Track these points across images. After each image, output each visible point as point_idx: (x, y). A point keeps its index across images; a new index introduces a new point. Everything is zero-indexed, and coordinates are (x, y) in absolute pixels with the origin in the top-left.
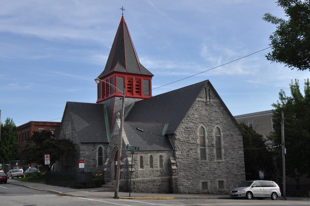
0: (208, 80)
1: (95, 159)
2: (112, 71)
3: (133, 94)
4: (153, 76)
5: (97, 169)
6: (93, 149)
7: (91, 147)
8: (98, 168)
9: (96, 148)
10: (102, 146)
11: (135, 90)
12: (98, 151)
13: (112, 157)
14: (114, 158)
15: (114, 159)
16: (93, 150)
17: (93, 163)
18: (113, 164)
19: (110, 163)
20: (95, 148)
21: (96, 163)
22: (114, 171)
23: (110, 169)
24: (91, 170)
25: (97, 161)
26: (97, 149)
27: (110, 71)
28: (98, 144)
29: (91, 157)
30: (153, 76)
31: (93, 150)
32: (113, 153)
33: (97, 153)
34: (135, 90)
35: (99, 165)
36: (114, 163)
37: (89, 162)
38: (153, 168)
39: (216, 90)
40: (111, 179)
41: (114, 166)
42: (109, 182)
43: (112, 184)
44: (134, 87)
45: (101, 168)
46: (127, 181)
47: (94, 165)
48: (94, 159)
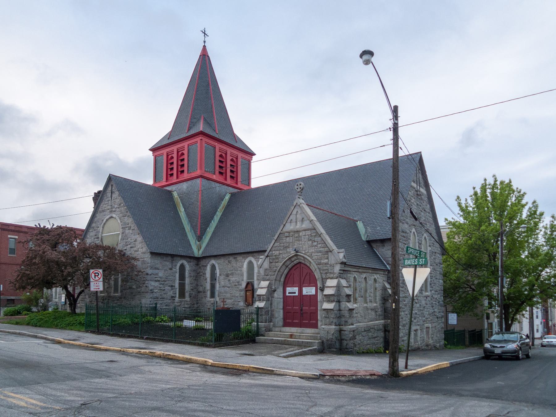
0: (421, 152)
1: (174, 286)
2: (192, 132)
3: (226, 179)
4: (255, 154)
5: (177, 304)
6: (170, 267)
7: (168, 263)
8: (178, 303)
9: (176, 266)
10: (185, 262)
11: (229, 174)
12: (178, 271)
13: (278, 279)
14: (282, 280)
15: (282, 282)
16: (171, 269)
17: (171, 293)
18: (279, 294)
19: (271, 291)
20: (174, 264)
21: (176, 294)
22: (282, 307)
23: (271, 304)
24: (166, 306)
25: (178, 290)
26: (178, 267)
27: (189, 130)
28: (179, 258)
29: (167, 282)
30: (255, 154)
31: (171, 269)
32: (282, 271)
33: (177, 275)
34: (229, 174)
35: (180, 297)
36: (282, 290)
37: (164, 290)
38: (367, 303)
39: (427, 173)
40: (274, 326)
41: (282, 296)
42: (270, 330)
43: (293, 337)
44: (229, 168)
45: (183, 303)
46: (341, 331)
47: (172, 297)
48: (172, 286)
